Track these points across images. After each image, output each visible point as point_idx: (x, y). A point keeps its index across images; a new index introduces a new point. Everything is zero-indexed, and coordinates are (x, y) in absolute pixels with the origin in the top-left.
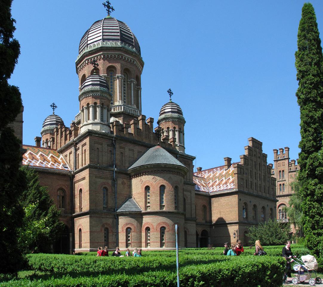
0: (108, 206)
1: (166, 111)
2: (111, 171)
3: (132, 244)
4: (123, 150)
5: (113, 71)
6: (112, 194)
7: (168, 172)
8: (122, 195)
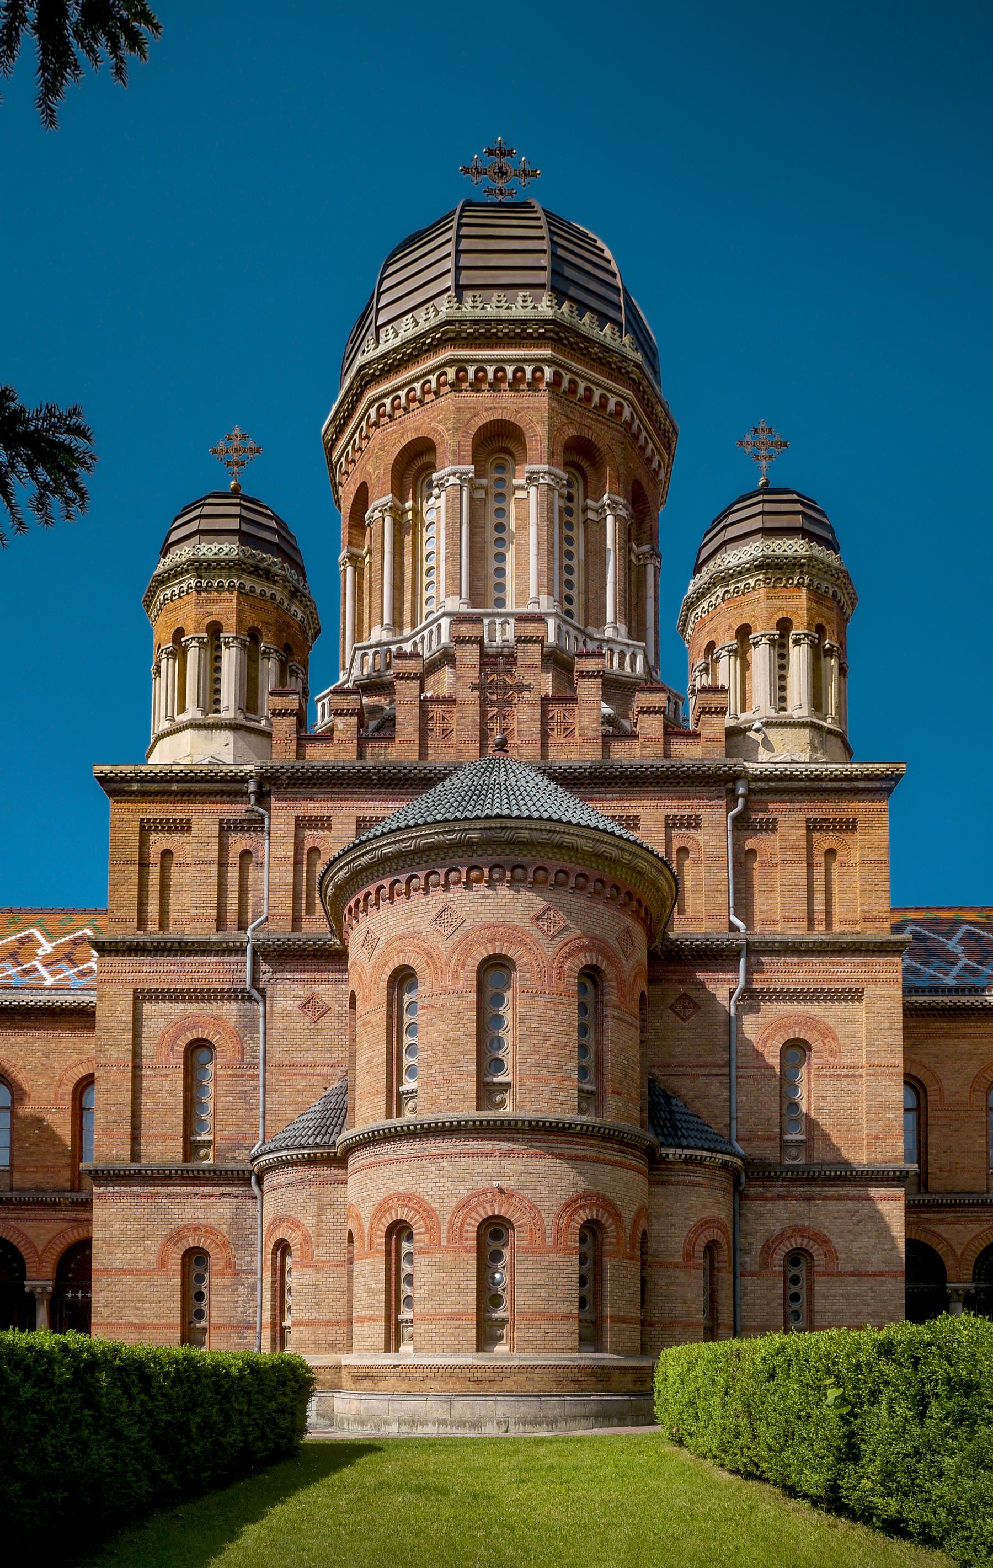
6: (238, 1072)
8: (304, 1070)
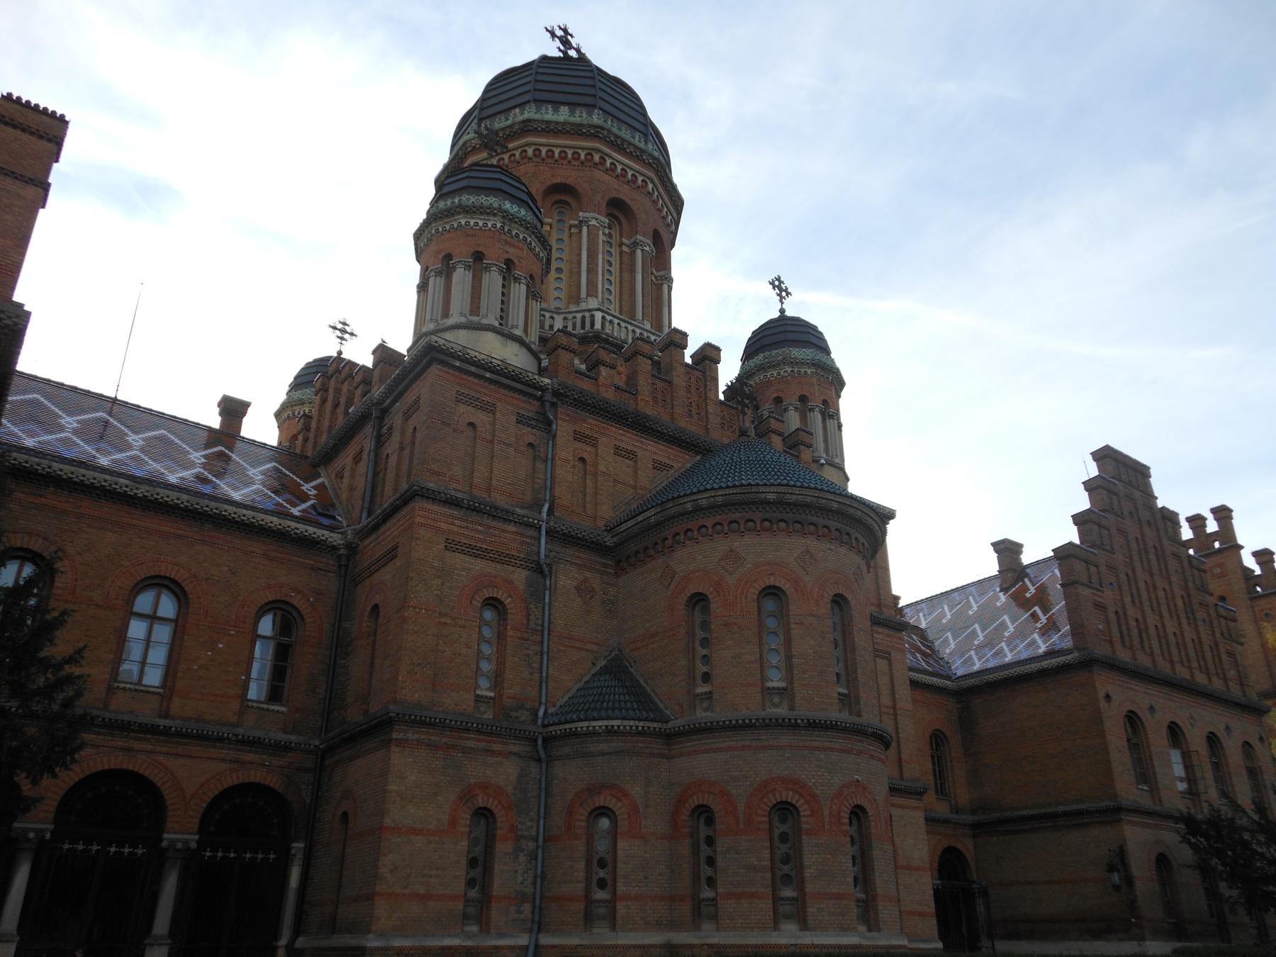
1: (767, 341)
2: (527, 525)
4: (589, 448)
5: (569, 204)
7: (798, 526)
8: (578, 644)
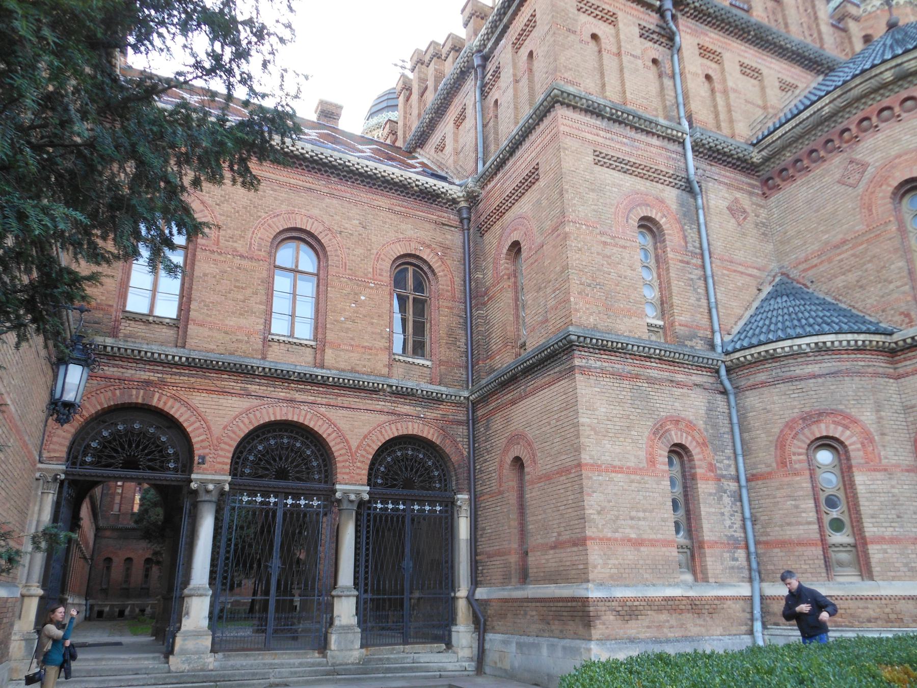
0: (672, 324)
3: (873, 549)
4: (714, 65)
6: (686, 259)
8: (741, 269)
